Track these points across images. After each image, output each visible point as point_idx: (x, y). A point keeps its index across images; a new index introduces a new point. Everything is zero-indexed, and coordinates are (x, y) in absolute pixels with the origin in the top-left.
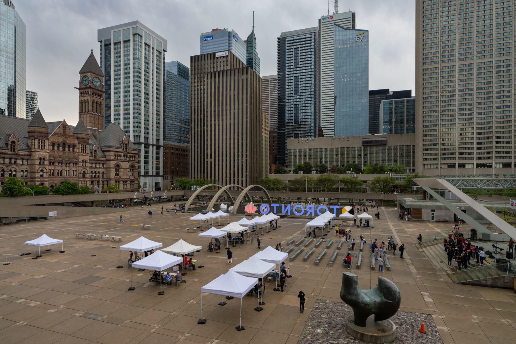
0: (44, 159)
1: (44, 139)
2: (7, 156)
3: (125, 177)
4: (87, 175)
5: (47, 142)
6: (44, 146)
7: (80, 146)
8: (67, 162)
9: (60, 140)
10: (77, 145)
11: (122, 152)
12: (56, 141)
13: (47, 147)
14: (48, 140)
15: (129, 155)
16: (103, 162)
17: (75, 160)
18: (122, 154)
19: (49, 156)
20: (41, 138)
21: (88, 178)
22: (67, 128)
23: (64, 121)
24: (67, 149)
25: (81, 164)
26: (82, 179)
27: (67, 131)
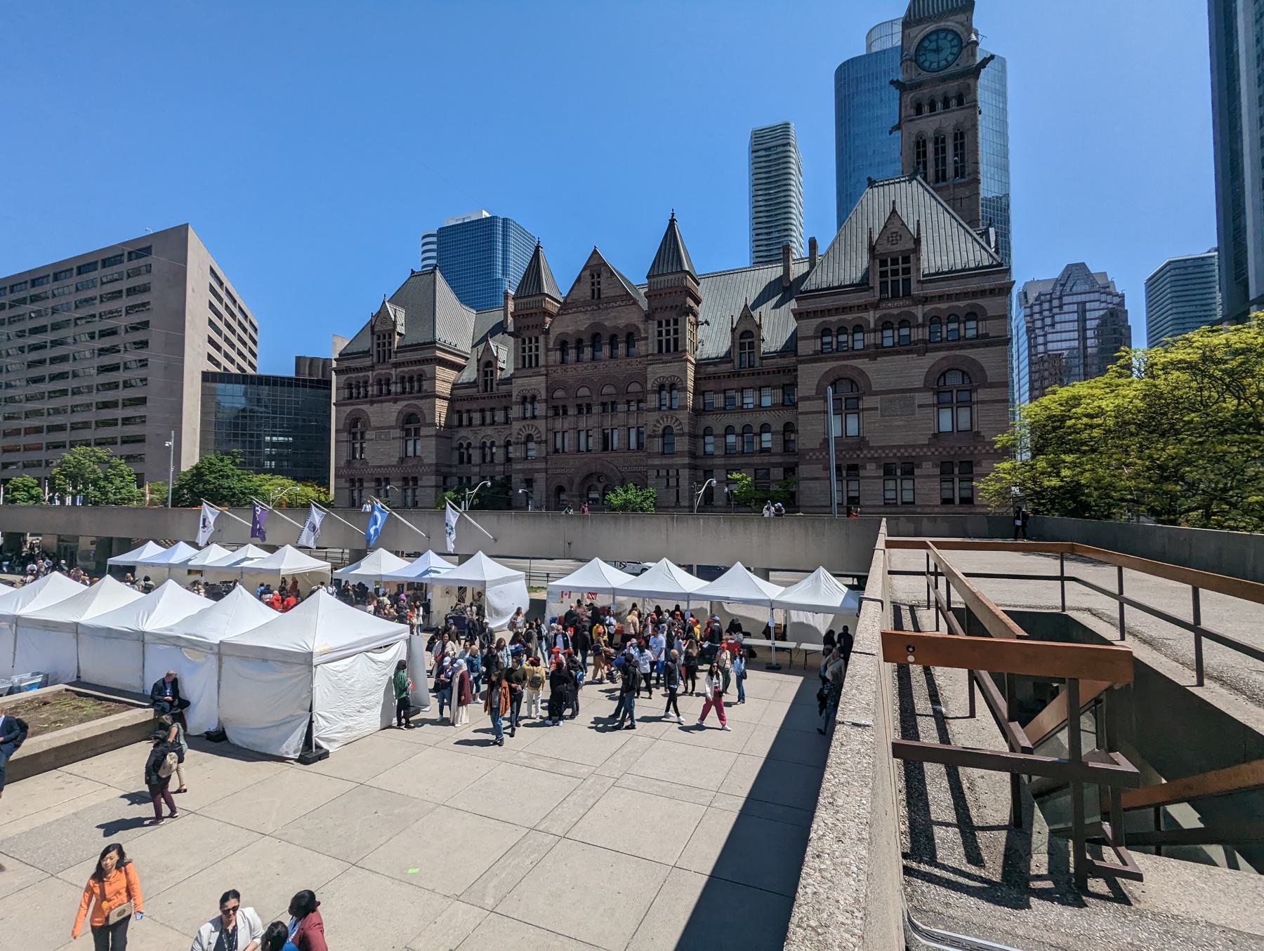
0: (534, 398)
1: (536, 332)
2: (474, 406)
3: (897, 439)
4: (682, 444)
5: (541, 339)
6: (537, 356)
7: (653, 327)
8: (584, 402)
9: (578, 323)
10: (641, 326)
11: (865, 308)
12: (570, 329)
13: (542, 362)
14: (547, 332)
15: (919, 312)
16: (786, 380)
17: (634, 388)
18: (871, 317)
19: (550, 389)
20: (526, 334)
21: (680, 454)
22: (604, 275)
23: (595, 252)
24: (606, 350)
25: (653, 400)
26: (657, 462)
27: (602, 280)
